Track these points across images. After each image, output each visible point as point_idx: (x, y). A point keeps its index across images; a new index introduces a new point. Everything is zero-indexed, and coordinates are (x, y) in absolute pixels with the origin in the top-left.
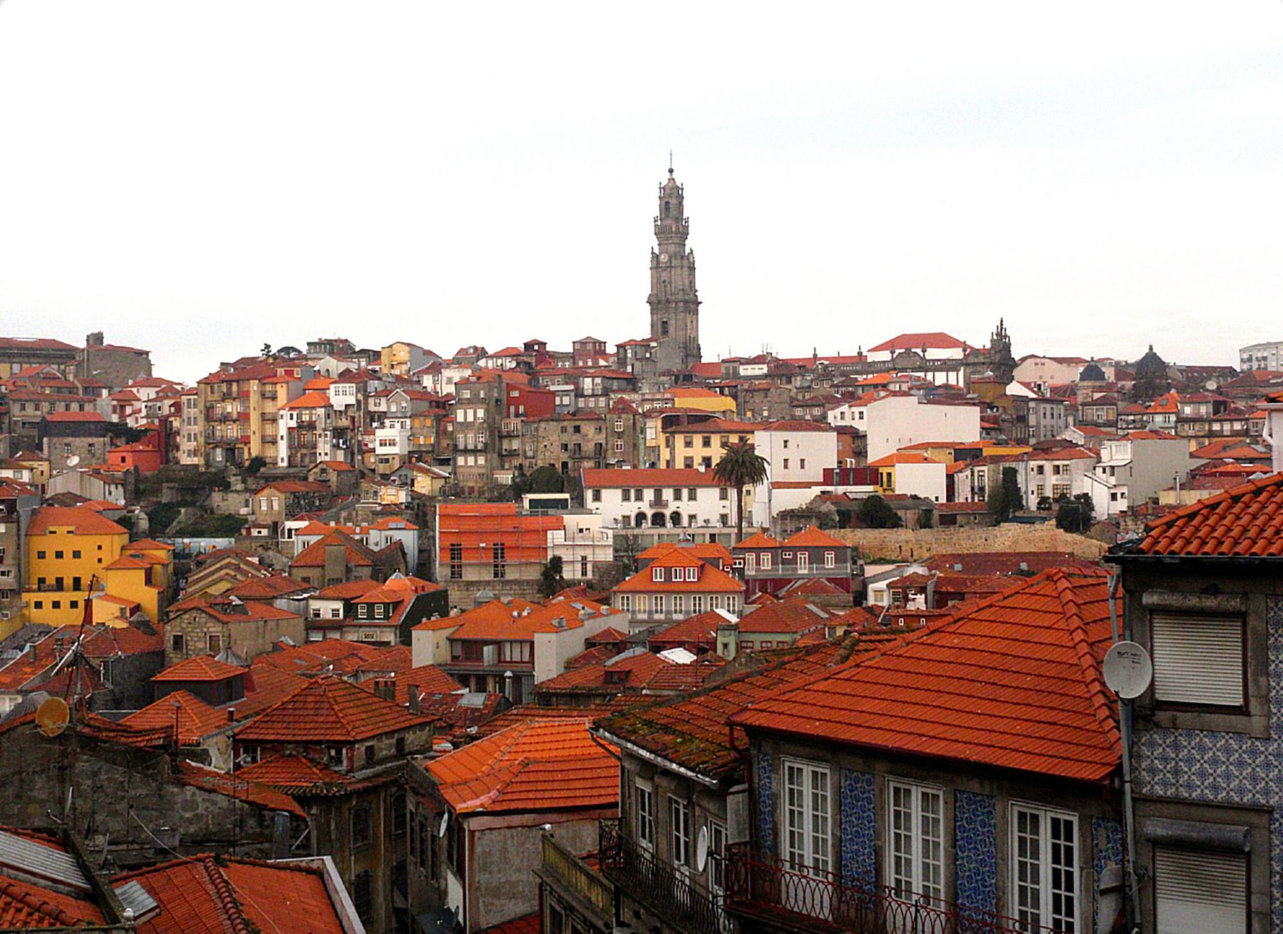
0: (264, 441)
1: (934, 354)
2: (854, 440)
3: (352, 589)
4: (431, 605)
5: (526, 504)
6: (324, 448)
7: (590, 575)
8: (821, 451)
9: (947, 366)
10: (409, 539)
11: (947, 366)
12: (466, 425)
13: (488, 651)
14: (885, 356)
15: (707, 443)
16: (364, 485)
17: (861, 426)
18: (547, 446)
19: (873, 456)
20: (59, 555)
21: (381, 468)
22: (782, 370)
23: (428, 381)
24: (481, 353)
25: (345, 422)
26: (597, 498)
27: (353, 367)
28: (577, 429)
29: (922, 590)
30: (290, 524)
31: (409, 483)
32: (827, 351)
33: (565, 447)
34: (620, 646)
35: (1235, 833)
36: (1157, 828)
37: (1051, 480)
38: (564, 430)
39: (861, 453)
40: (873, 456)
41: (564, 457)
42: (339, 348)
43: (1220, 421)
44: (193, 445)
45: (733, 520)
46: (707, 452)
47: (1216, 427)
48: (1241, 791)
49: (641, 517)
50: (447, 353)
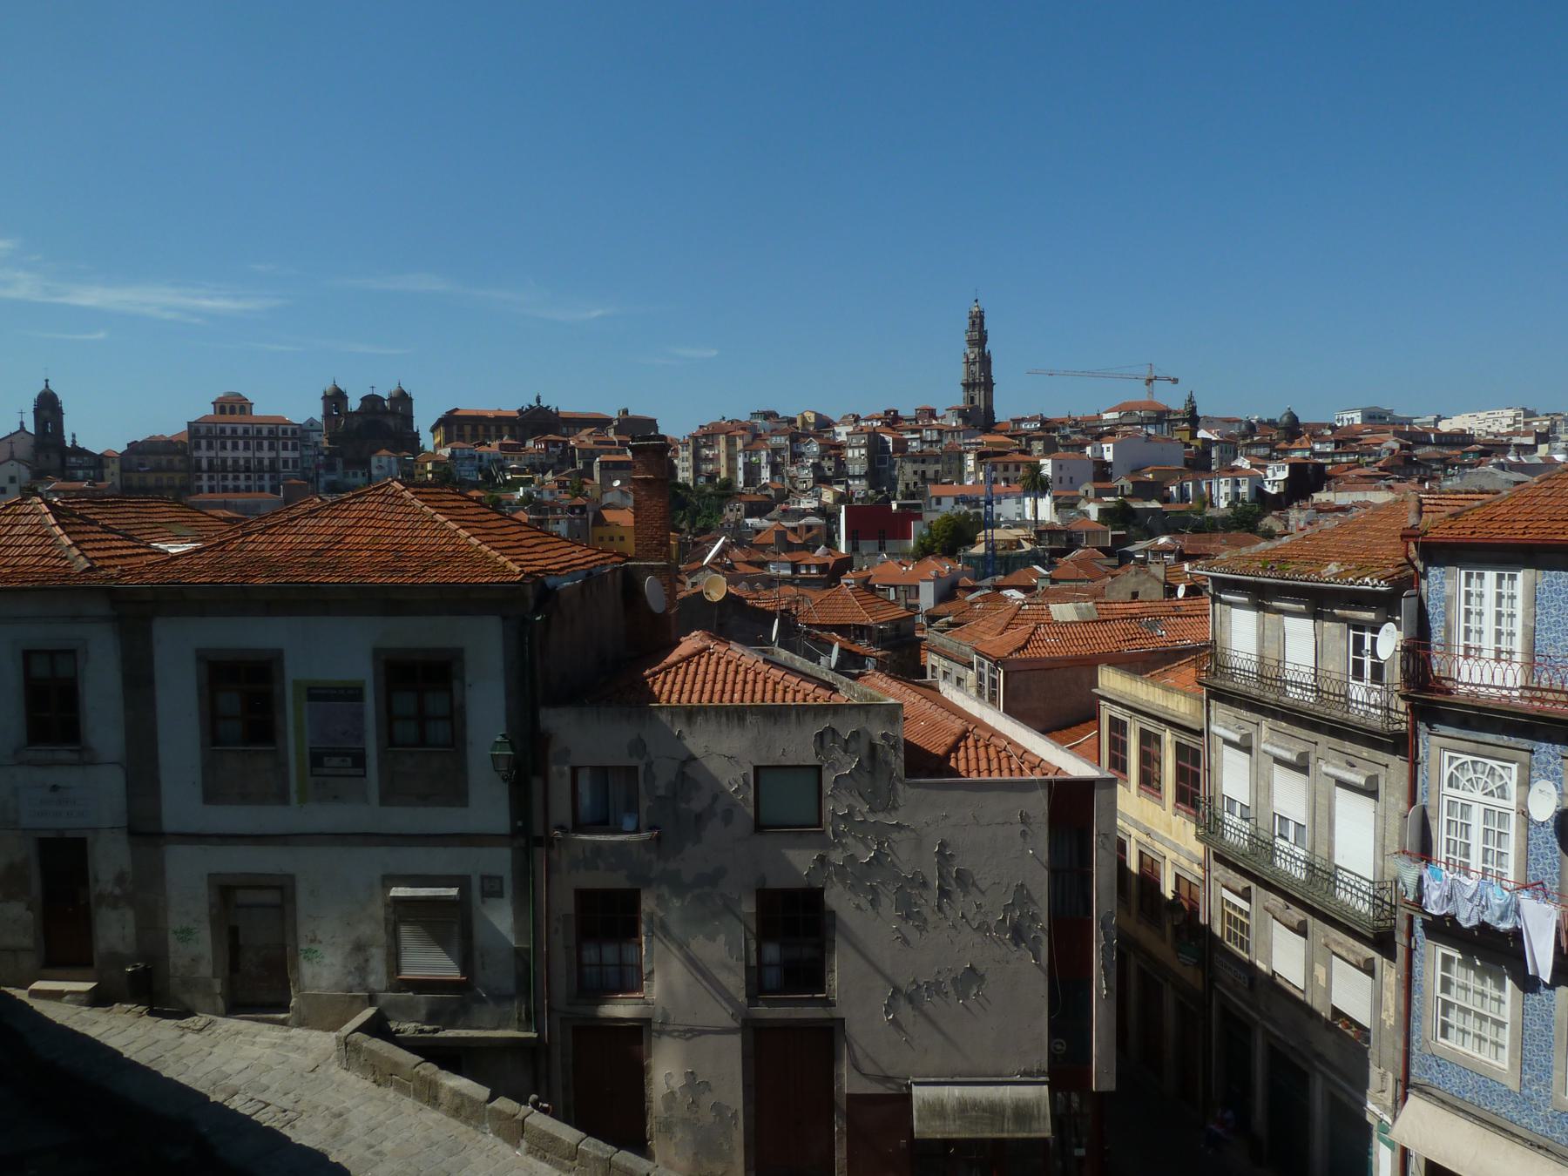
0: (729, 469)
3: (796, 556)
4: (845, 565)
5: (894, 506)
6: (766, 475)
14: (1115, 415)
15: (1006, 469)
20: (612, 539)
24: (857, 419)
26: (939, 502)
29: (1171, 552)
30: (749, 521)
31: (819, 496)
32: (1078, 415)
33: (915, 473)
34: (973, 589)
43: (1341, 454)
44: (686, 474)
45: (1029, 515)
46: (1007, 474)
47: (1337, 459)
50: (835, 416)
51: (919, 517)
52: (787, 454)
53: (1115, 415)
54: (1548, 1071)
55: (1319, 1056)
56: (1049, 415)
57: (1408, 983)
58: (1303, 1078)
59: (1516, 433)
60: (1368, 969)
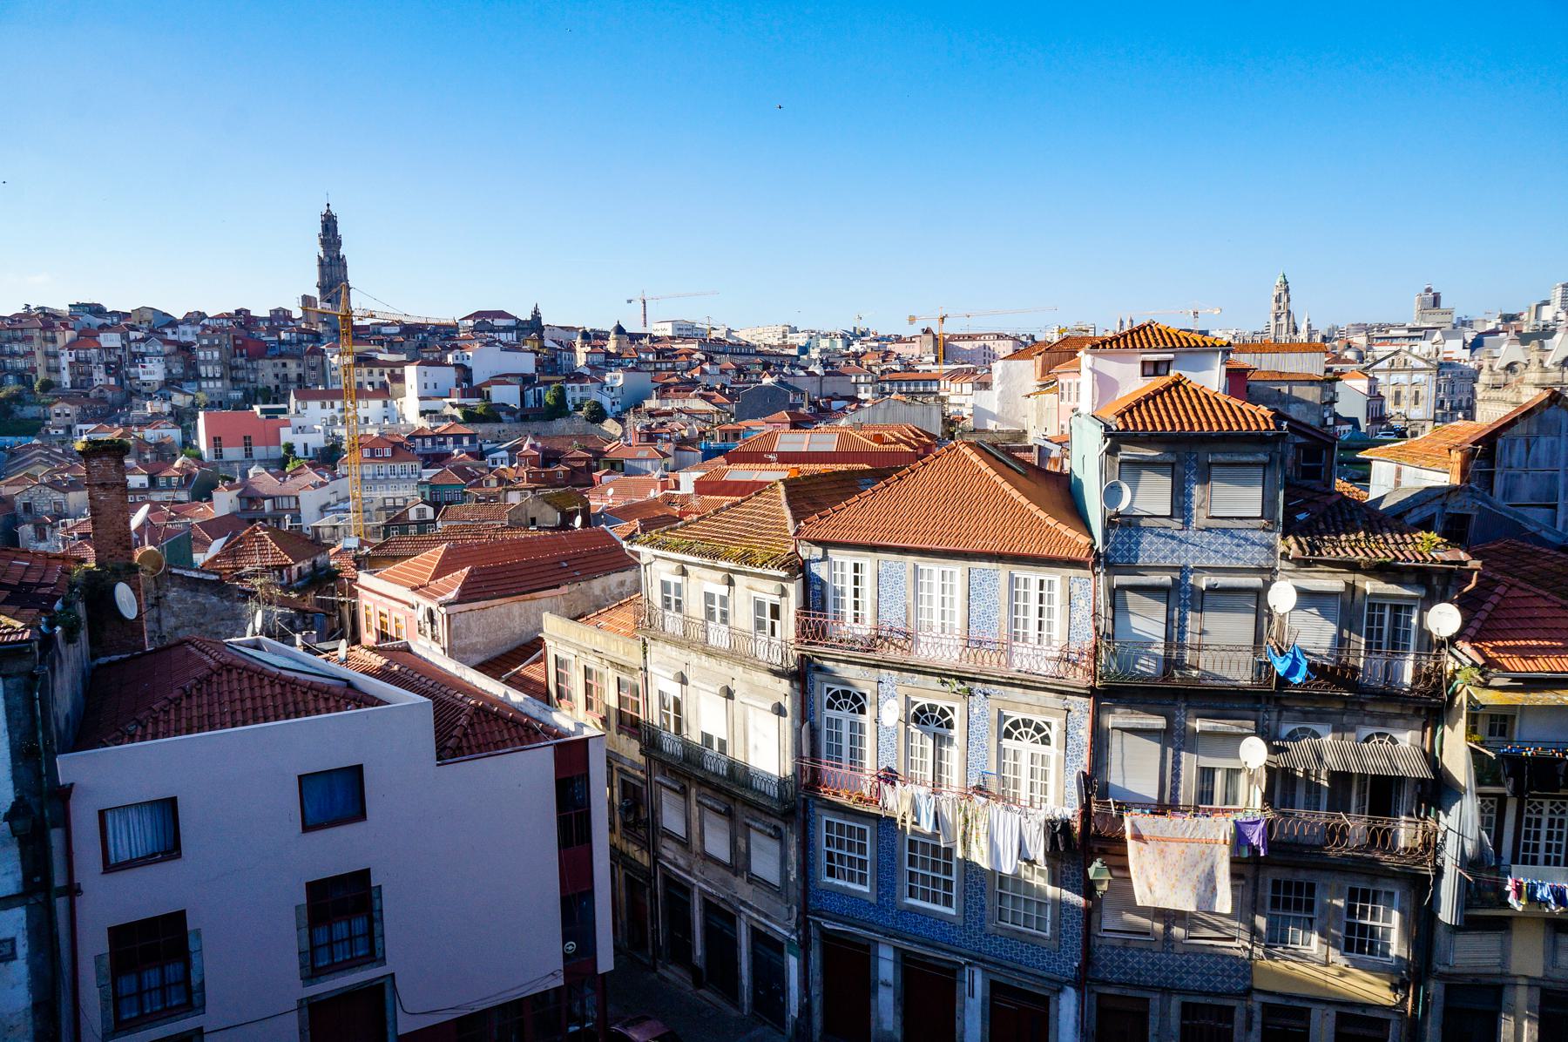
0: (48, 369)
1: (499, 322)
2: (465, 373)
6: (99, 376)
7: (310, 454)
8: (448, 376)
9: (507, 329)
10: (176, 434)
11: (507, 329)
12: (206, 362)
13: (267, 504)
14: (470, 323)
15: (371, 373)
16: (135, 400)
17: (469, 364)
18: (266, 372)
19: (476, 381)
21: (145, 389)
22: (409, 330)
23: (169, 331)
24: (203, 316)
25: (113, 359)
27: (108, 322)
28: (284, 365)
30: (79, 427)
33: (276, 376)
35: (1166, 579)
36: (1120, 580)
37: (578, 395)
38: (275, 365)
39: (469, 380)
40: (476, 381)
41: (277, 382)
42: (97, 310)
46: (371, 379)
48: (1165, 558)
49: (334, 419)
50: (179, 316)
51: (287, 424)
52: (126, 356)
53: (470, 323)
54: (893, 886)
55: (743, 903)
56: (407, 321)
57: (806, 846)
58: (731, 919)
59: (784, 346)
60: (778, 836)
